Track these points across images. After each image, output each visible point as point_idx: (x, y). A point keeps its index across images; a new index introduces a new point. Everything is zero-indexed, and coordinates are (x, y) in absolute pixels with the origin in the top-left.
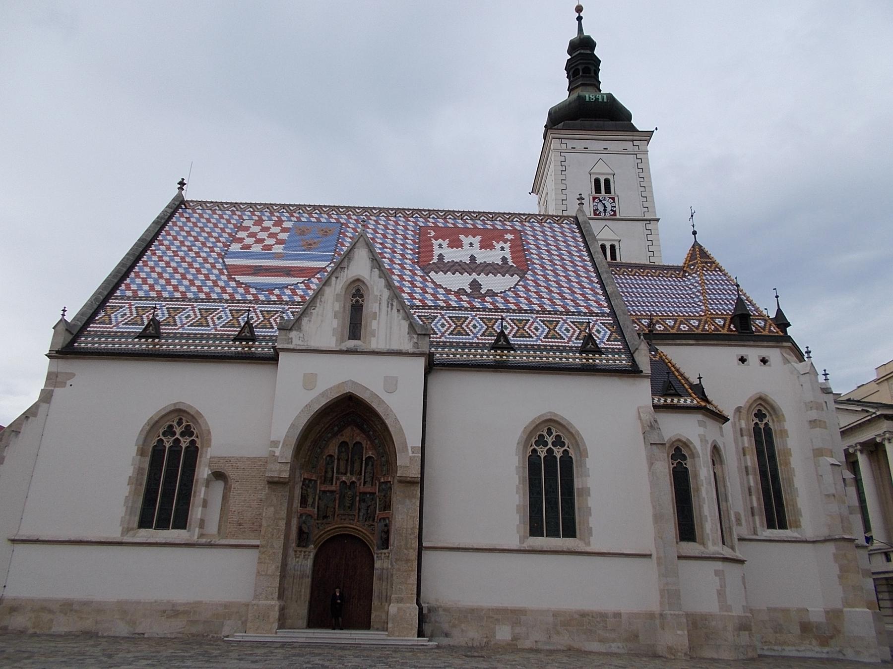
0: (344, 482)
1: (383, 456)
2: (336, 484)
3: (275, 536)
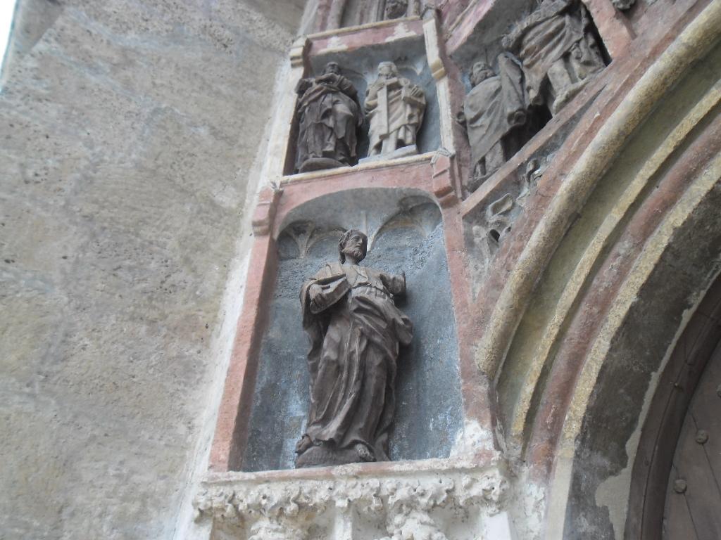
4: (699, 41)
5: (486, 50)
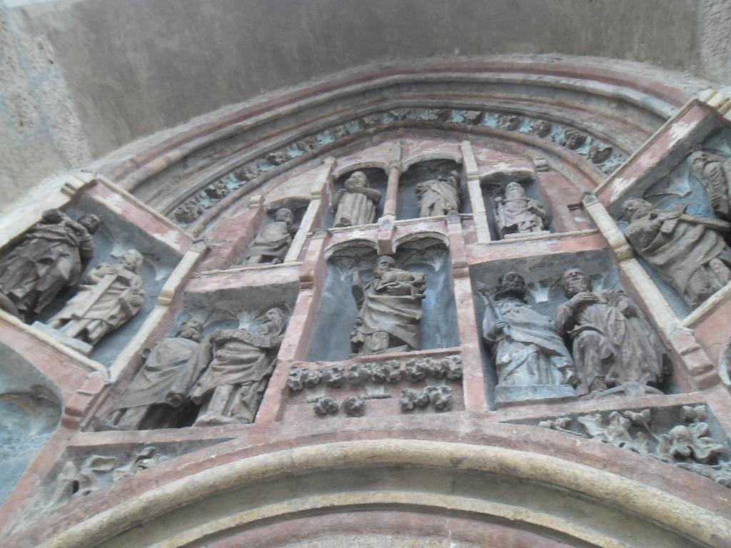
4: (301, 464)
5: (212, 311)
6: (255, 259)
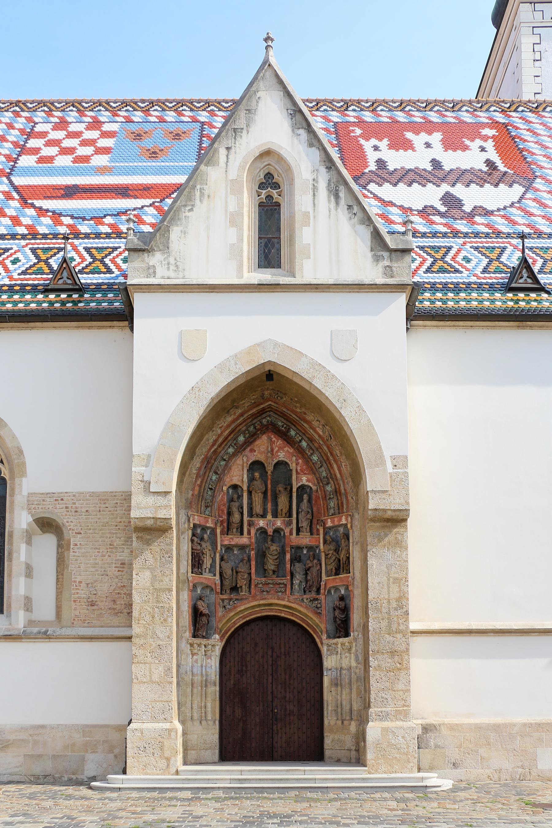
0: (263, 531)
1: (328, 484)
2: (249, 533)
3: (157, 618)
6: (235, 530)
